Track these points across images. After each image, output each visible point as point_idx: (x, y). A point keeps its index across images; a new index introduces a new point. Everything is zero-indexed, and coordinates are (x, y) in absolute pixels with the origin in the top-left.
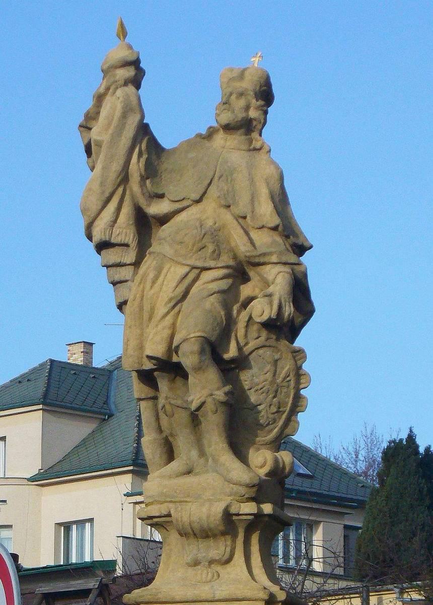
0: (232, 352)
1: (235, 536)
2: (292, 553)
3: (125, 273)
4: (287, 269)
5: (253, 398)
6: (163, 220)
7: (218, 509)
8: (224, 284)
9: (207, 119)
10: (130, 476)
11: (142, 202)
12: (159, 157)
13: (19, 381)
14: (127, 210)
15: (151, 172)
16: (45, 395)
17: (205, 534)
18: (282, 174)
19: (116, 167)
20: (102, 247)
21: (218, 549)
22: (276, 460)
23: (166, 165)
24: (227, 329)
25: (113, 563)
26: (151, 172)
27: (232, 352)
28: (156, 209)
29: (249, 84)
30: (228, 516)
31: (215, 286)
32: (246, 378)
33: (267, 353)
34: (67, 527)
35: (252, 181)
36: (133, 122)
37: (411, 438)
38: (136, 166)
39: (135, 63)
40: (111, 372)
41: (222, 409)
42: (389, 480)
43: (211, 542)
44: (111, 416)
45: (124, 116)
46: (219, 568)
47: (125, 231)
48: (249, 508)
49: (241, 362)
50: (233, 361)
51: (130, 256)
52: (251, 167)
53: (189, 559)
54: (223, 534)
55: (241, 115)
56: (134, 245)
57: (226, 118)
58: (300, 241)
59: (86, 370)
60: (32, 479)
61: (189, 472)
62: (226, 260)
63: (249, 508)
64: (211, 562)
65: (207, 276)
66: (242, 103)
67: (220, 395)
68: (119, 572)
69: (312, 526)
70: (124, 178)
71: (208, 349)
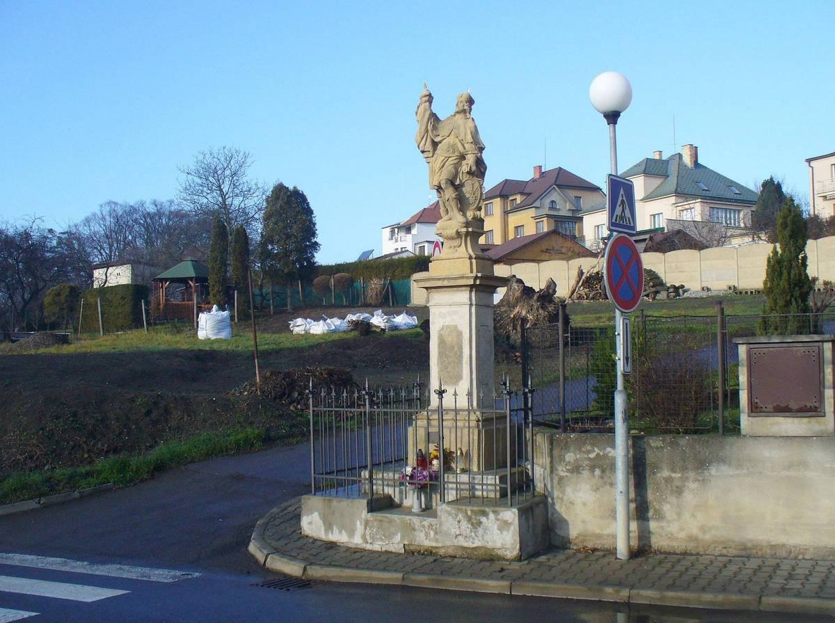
0: (458, 182)
1: (461, 238)
2: (732, 221)
3: (429, 160)
4: (474, 155)
5: (467, 196)
6: (440, 142)
7: (454, 231)
8: (455, 162)
9: (453, 109)
10: (674, 197)
11: (432, 137)
12: (438, 123)
13: (636, 166)
14: (429, 140)
15: (435, 128)
16: (645, 170)
17: (452, 238)
18: (631, 99)
19: (424, 128)
20: (423, 152)
21: (457, 242)
22: (474, 215)
23: (440, 125)
24: (456, 175)
25: (663, 228)
26: (435, 128)
27: (458, 182)
28: (437, 140)
29: (464, 98)
30: (458, 233)
31: (452, 163)
32: (464, 189)
33: (470, 182)
34: (654, 216)
35: (465, 128)
36: (428, 113)
37: (772, 179)
38: (430, 128)
39: (430, 95)
40: (668, 161)
41: (455, 200)
42: (764, 195)
43: (454, 241)
44: (668, 176)
45: (425, 112)
46: (458, 249)
47: (429, 147)
48: (465, 230)
49: (462, 185)
50: (458, 185)
51: (431, 155)
52: (465, 124)
53: (449, 246)
54: (458, 238)
55: (461, 108)
56: (431, 151)
57: (457, 110)
58: (481, 145)
59: (660, 161)
60: (641, 200)
61: (450, 219)
62: (457, 154)
63: (465, 230)
64: (455, 247)
65: (450, 159)
66: (462, 104)
67: (454, 196)
68: (666, 231)
69: (739, 211)
70: (427, 131)
71: (449, 182)
